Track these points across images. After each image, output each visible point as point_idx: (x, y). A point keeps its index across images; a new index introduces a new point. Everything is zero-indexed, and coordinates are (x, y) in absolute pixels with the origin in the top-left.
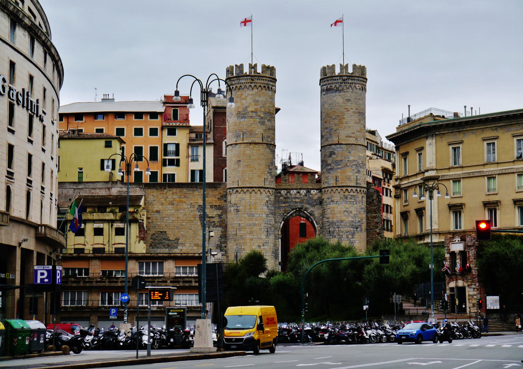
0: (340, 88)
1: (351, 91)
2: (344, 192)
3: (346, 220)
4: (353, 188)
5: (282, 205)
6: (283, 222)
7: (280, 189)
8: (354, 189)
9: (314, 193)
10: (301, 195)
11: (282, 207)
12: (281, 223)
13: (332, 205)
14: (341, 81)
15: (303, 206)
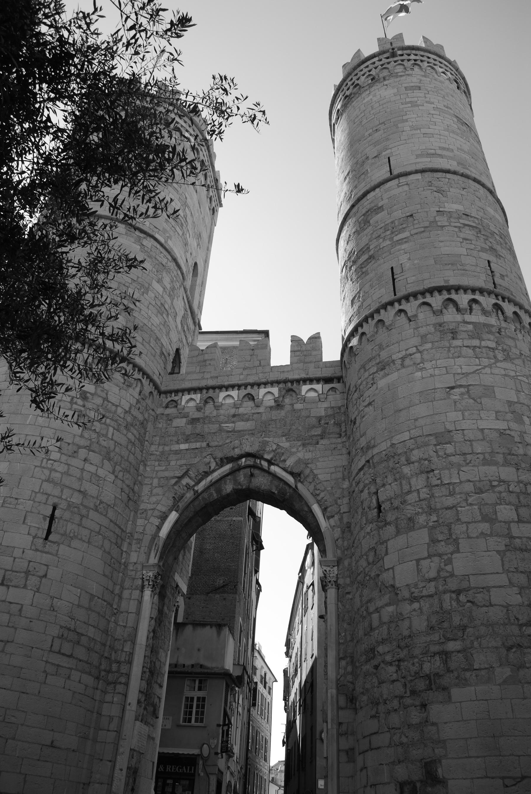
0: (385, 73)
1: (423, 74)
2: (438, 313)
3: (466, 425)
4: (477, 297)
5: (175, 447)
6: (173, 516)
7: (177, 392)
8: (487, 302)
9: (312, 394)
10: (258, 406)
11: (177, 452)
12: (164, 518)
13: (382, 383)
14: (384, 61)
15: (265, 443)
